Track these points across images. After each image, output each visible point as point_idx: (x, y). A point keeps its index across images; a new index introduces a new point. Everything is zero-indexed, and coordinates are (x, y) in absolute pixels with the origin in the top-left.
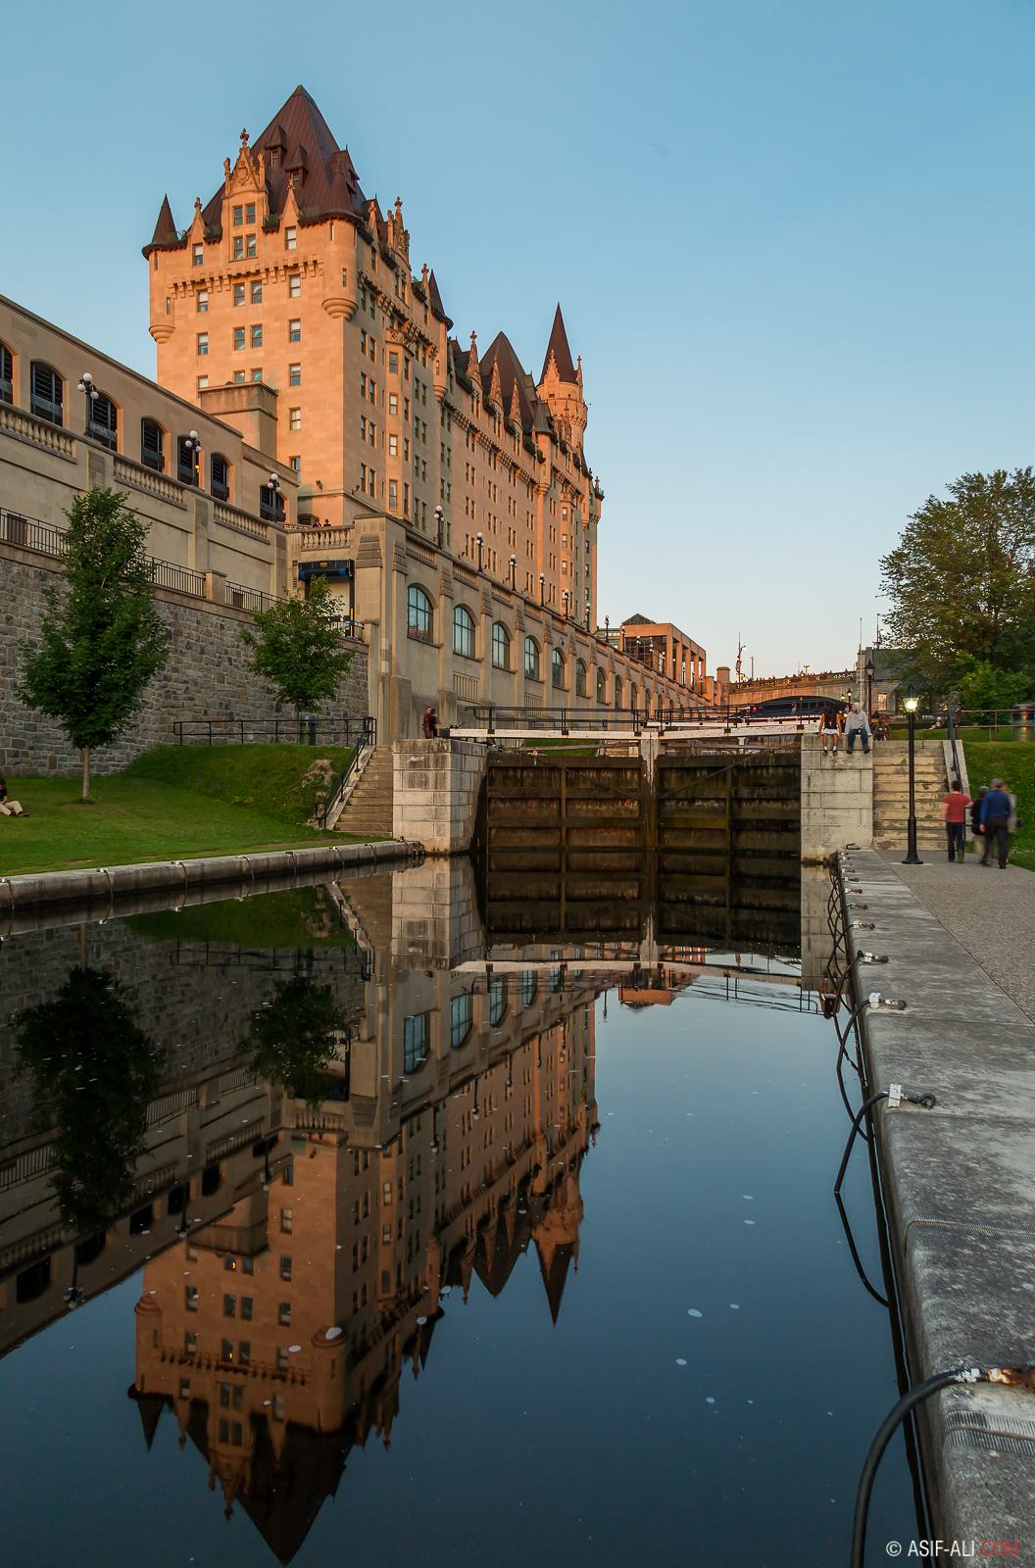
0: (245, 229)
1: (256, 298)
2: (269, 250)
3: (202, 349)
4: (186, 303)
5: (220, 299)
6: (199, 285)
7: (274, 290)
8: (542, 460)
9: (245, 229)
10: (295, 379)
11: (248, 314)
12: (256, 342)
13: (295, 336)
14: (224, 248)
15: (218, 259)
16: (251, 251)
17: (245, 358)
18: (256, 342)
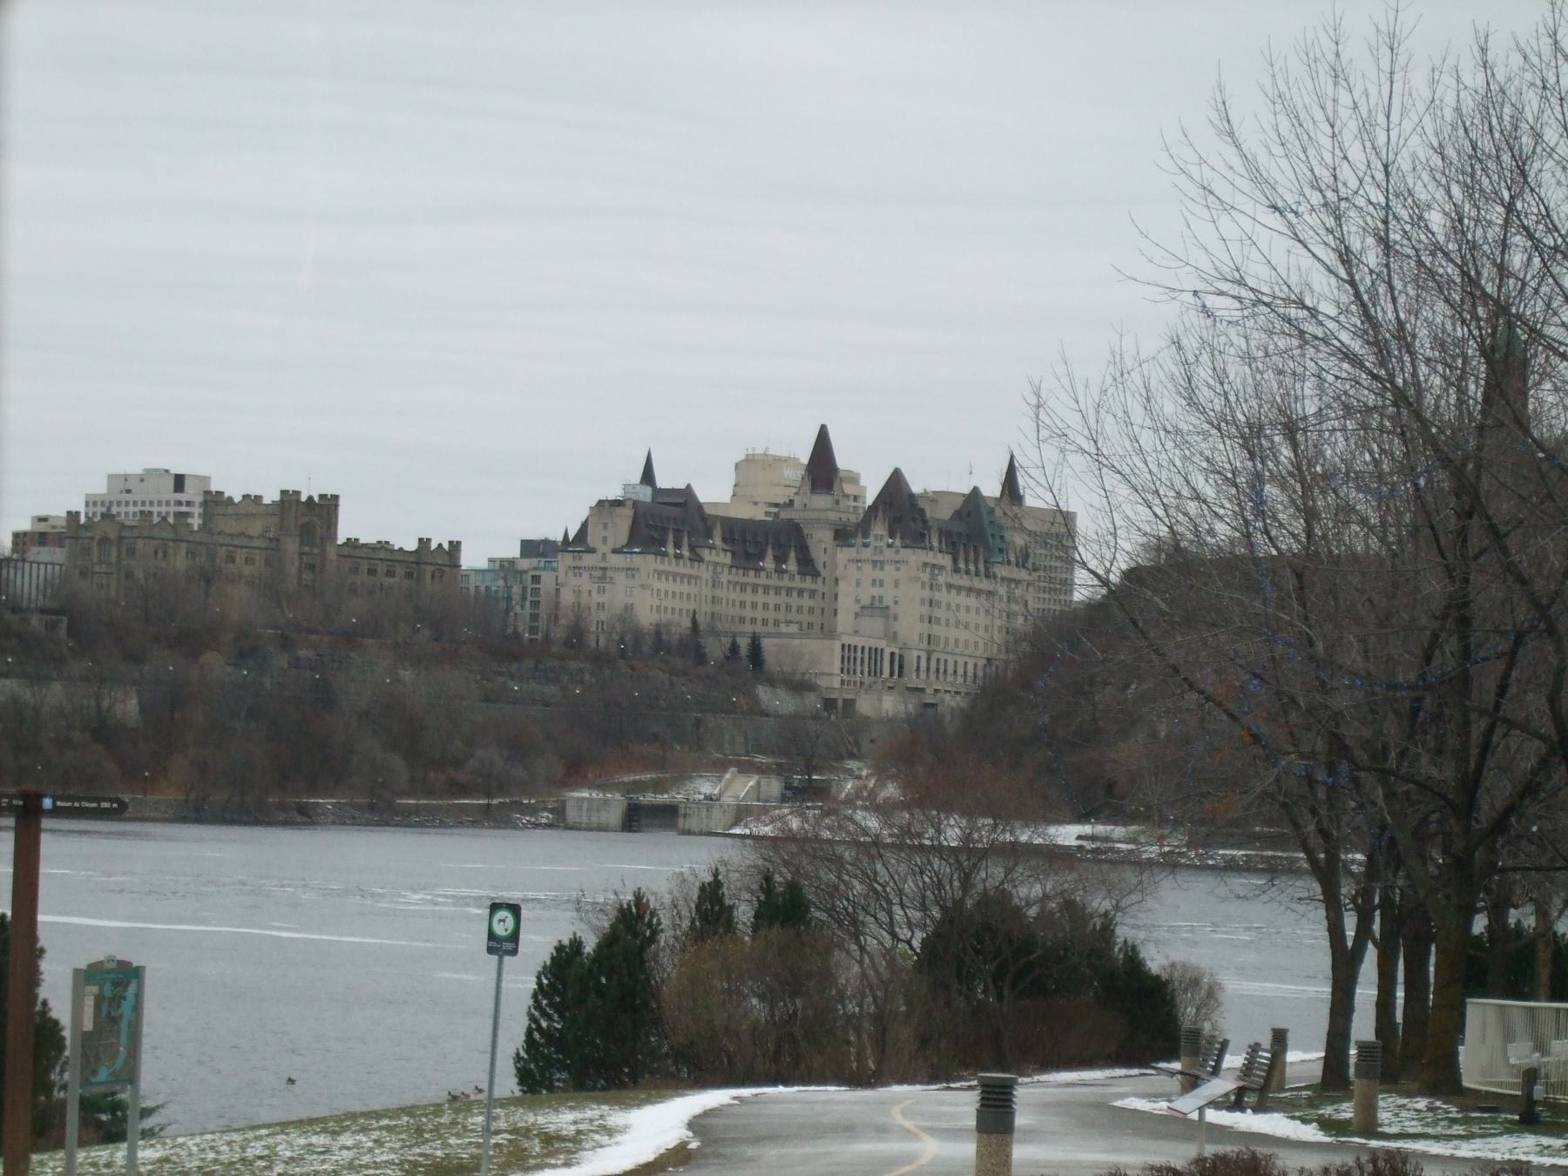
0: (879, 544)
1: (882, 569)
2: (889, 554)
3: (858, 584)
4: (852, 568)
5: (867, 568)
6: (858, 561)
7: (889, 568)
8: (995, 577)
9: (879, 544)
10: (896, 602)
11: (878, 575)
12: (881, 585)
13: (896, 584)
14: (870, 549)
15: (867, 553)
16: (881, 552)
17: (876, 591)
18: (881, 585)
